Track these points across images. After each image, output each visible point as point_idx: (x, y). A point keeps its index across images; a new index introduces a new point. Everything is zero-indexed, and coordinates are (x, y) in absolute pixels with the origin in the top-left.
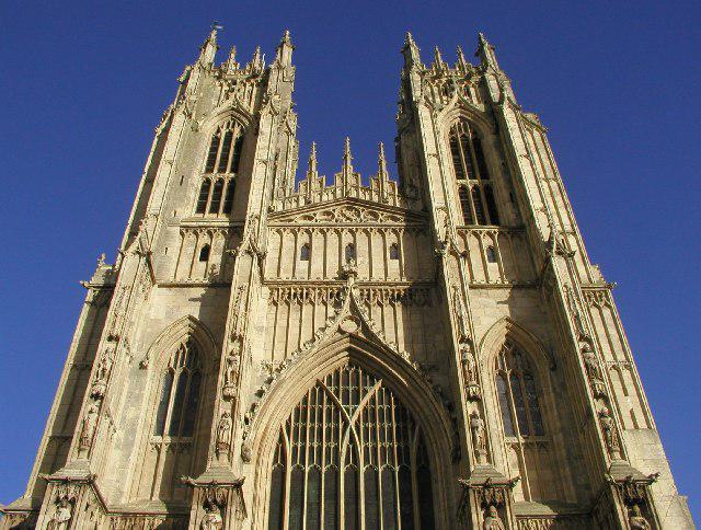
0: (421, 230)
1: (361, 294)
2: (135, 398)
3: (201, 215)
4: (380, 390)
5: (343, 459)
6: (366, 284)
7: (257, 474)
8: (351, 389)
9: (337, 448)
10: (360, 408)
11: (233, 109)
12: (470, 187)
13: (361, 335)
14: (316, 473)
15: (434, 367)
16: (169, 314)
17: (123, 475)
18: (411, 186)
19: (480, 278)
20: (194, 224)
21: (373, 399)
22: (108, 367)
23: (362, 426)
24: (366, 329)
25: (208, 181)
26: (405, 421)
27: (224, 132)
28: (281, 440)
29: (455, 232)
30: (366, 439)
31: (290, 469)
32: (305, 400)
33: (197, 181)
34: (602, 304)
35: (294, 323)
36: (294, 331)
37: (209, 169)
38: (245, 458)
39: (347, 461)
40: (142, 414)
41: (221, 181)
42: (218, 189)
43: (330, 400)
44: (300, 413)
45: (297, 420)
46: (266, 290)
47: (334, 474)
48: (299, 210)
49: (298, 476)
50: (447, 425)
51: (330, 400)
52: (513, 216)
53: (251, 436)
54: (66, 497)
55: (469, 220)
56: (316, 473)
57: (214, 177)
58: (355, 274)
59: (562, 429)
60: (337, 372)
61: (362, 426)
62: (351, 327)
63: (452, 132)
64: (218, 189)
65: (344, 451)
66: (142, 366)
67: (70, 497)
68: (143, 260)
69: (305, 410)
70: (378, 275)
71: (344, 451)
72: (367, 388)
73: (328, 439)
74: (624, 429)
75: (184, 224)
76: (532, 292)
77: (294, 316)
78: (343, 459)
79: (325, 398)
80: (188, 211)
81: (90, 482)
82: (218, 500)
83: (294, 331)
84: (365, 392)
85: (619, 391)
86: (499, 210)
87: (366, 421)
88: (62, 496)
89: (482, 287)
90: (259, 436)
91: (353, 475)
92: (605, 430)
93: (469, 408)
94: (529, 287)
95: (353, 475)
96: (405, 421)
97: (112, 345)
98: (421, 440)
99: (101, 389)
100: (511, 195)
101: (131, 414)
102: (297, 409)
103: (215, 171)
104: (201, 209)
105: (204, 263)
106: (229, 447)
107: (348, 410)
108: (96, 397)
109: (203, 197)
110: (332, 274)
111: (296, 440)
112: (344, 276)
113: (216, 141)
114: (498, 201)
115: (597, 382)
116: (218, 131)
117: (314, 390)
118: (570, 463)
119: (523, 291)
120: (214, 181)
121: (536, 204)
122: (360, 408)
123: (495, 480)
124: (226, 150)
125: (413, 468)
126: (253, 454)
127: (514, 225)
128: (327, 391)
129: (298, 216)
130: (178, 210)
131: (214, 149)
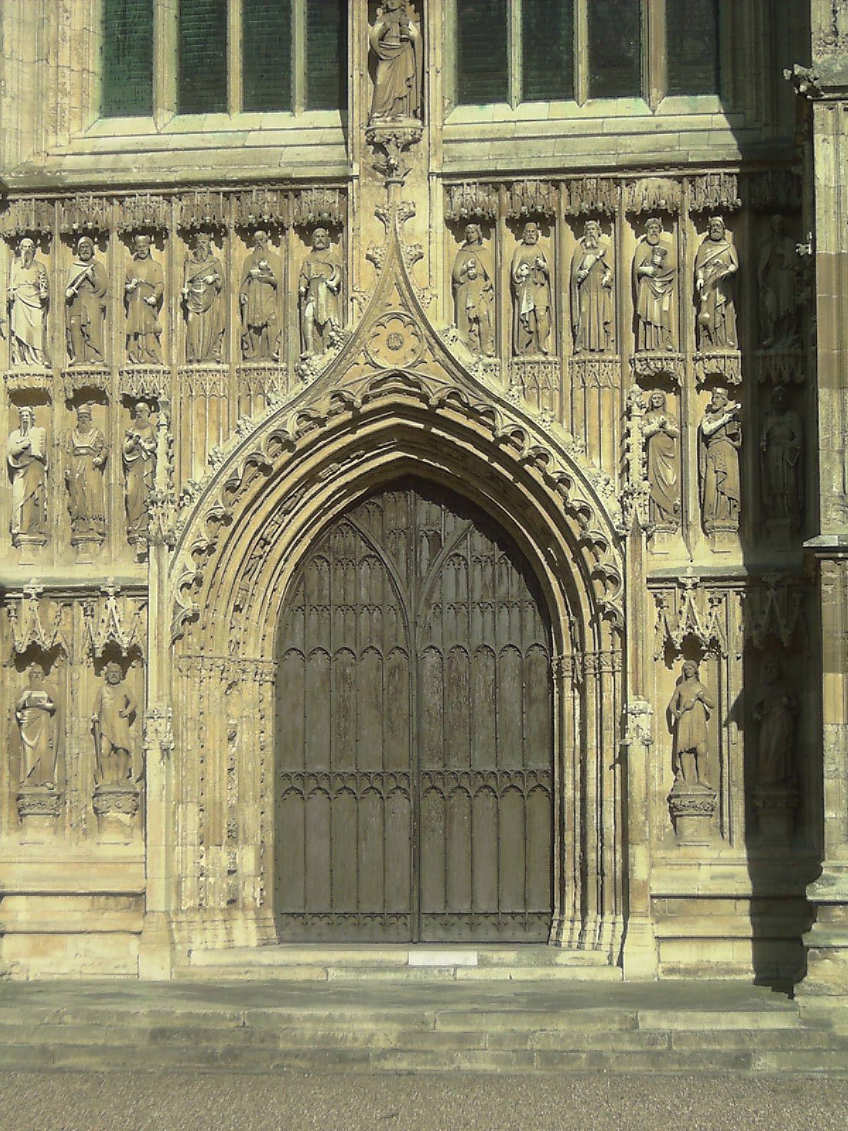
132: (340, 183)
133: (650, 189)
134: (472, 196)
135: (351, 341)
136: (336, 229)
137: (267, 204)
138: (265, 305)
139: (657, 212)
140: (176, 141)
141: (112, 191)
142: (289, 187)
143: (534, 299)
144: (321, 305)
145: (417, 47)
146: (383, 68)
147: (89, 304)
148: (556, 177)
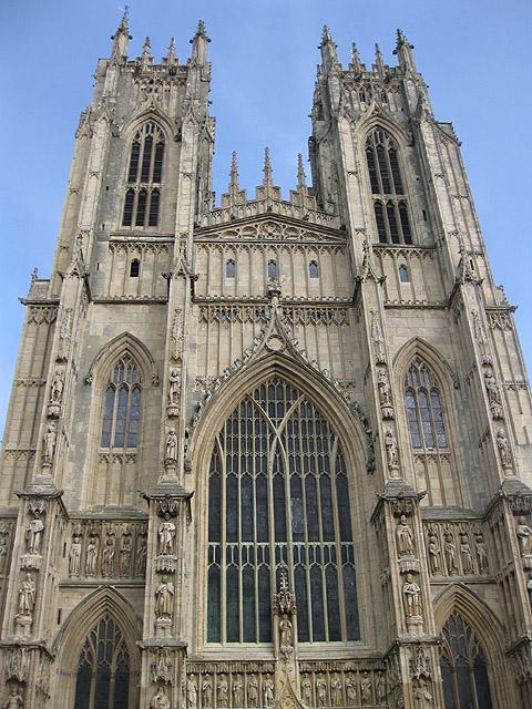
0: (339, 248)
1: (284, 313)
2: (82, 414)
3: (128, 228)
4: (302, 403)
5: (271, 467)
6: (289, 304)
7: (197, 482)
8: (276, 402)
9: (265, 457)
10: (285, 420)
11: (151, 111)
12: (385, 202)
13: (286, 353)
14: (247, 480)
15: (350, 383)
16: (107, 331)
17: (78, 485)
18: (330, 202)
19: (393, 297)
20: (122, 238)
21: (296, 412)
22: (60, 389)
23: (287, 438)
24: (289, 347)
25: (131, 191)
26: (325, 433)
27: (143, 136)
28: (216, 449)
29: (371, 249)
30: (291, 448)
31: (225, 476)
32: (236, 412)
33: (121, 190)
34: (503, 326)
35: (224, 340)
36: (224, 348)
37: (132, 180)
38: (187, 470)
39: (275, 470)
40: (90, 428)
41: (144, 191)
42: (142, 199)
43: (257, 412)
44: (232, 424)
45: (229, 432)
46: (196, 307)
47: (262, 480)
48: (224, 225)
49: (232, 481)
50: (363, 438)
51: (257, 412)
52: (425, 235)
53: (191, 448)
54: (37, 510)
55: (383, 238)
56: (247, 480)
57: (137, 185)
58: (280, 292)
59: (463, 443)
60: (263, 386)
61: (287, 438)
62: (276, 345)
63: (368, 142)
64: (142, 199)
65: (271, 459)
66: (87, 383)
67: (41, 509)
68: (82, 281)
69: (236, 421)
70: (300, 294)
71: (271, 459)
72: (291, 402)
73: (258, 449)
74: (517, 444)
75: (113, 238)
76: (441, 313)
77: (223, 333)
78: (271, 467)
79: (254, 411)
80: (114, 225)
81: (58, 497)
82: (171, 510)
83: (224, 348)
84: (289, 405)
85: (514, 410)
86: (412, 227)
87: (290, 433)
88: (34, 509)
89: (395, 307)
90: (197, 448)
91: (279, 481)
92: (500, 449)
93: (384, 428)
94: (438, 308)
95: (279, 481)
96: (325, 433)
97: (61, 367)
98: (339, 450)
99: (54, 410)
100: (424, 212)
101: (80, 428)
102: (229, 421)
103: (138, 180)
104: (127, 222)
105: (134, 280)
106: (176, 461)
107: (274, 422)
108: (52, 417)
109: (128, 207)
110: (259, 292)
111: (229, 449)
112: (270, 295)
113: (136, 146)
114: (411, 219)
115: (494, 404)
116: (138, 136)
117: (243, 403)
118: (468, 474)
119: (433, 312)
120: (137, 190)
121: (448, 228)
122: (285, 420)
123: (405, 494)
124: (147, 157)
125: (333, 476)
126: (193, 465)
127: (426, 244)
128: (255, 404)
129: (223, 232)
130: (106, 223)
131: (135, 156)
132: (273, 663)
133: (348, 665)
134: (306, 666)
135: (277, 703)
136: (272, 674)
137: (255, 667)
138: (255, 694)
139: (351, 671)
140: (229, 650)
141: (215, 663)
142: (260, 663)
143: (322, 693)
144: (269, 694)
145: (291, 629)
146: (283, 634)
147: (209, 692)
148: (326, 662)
